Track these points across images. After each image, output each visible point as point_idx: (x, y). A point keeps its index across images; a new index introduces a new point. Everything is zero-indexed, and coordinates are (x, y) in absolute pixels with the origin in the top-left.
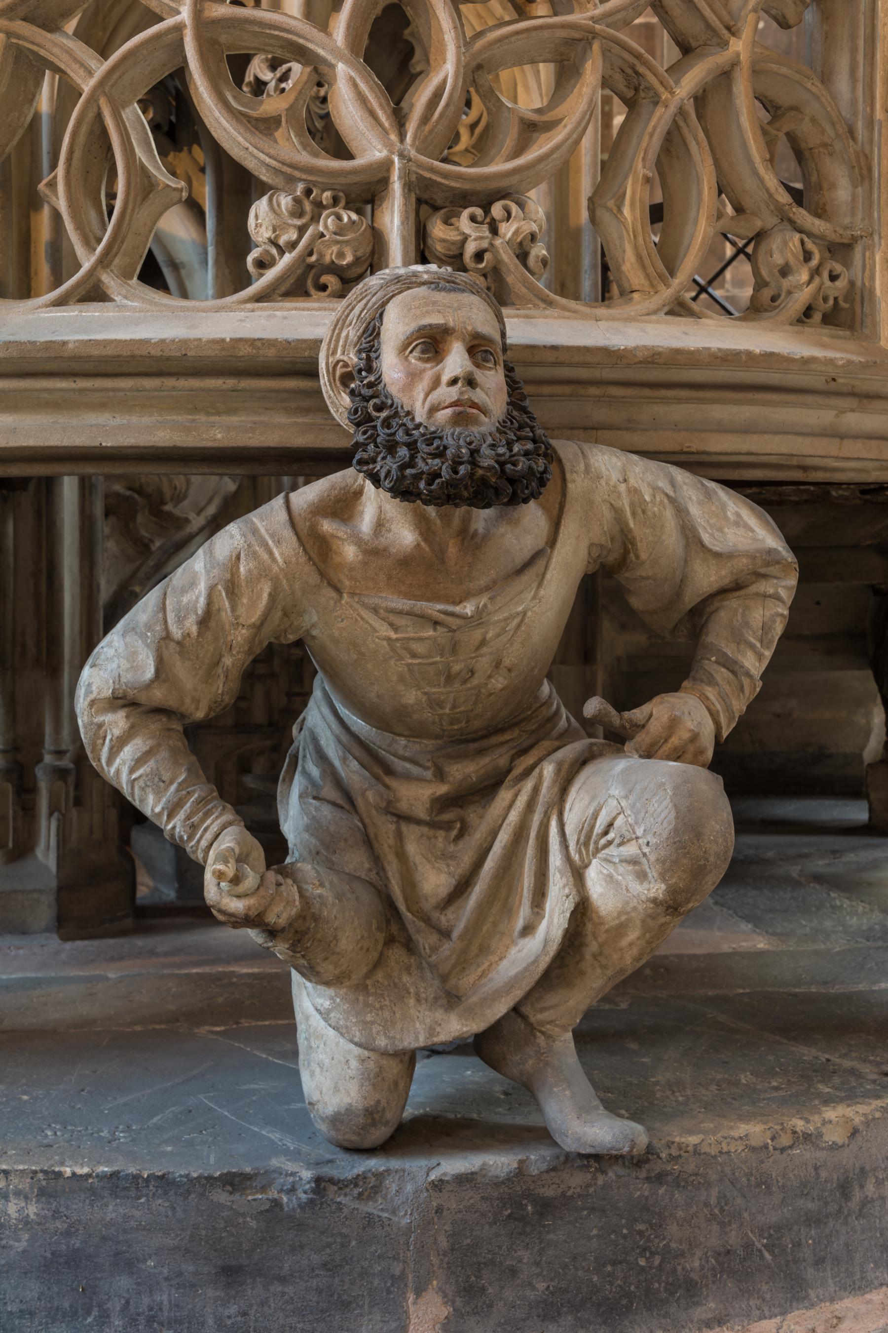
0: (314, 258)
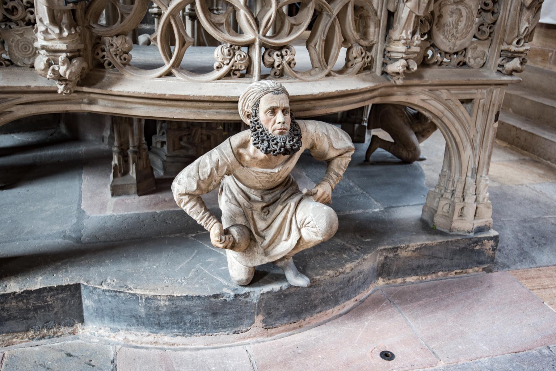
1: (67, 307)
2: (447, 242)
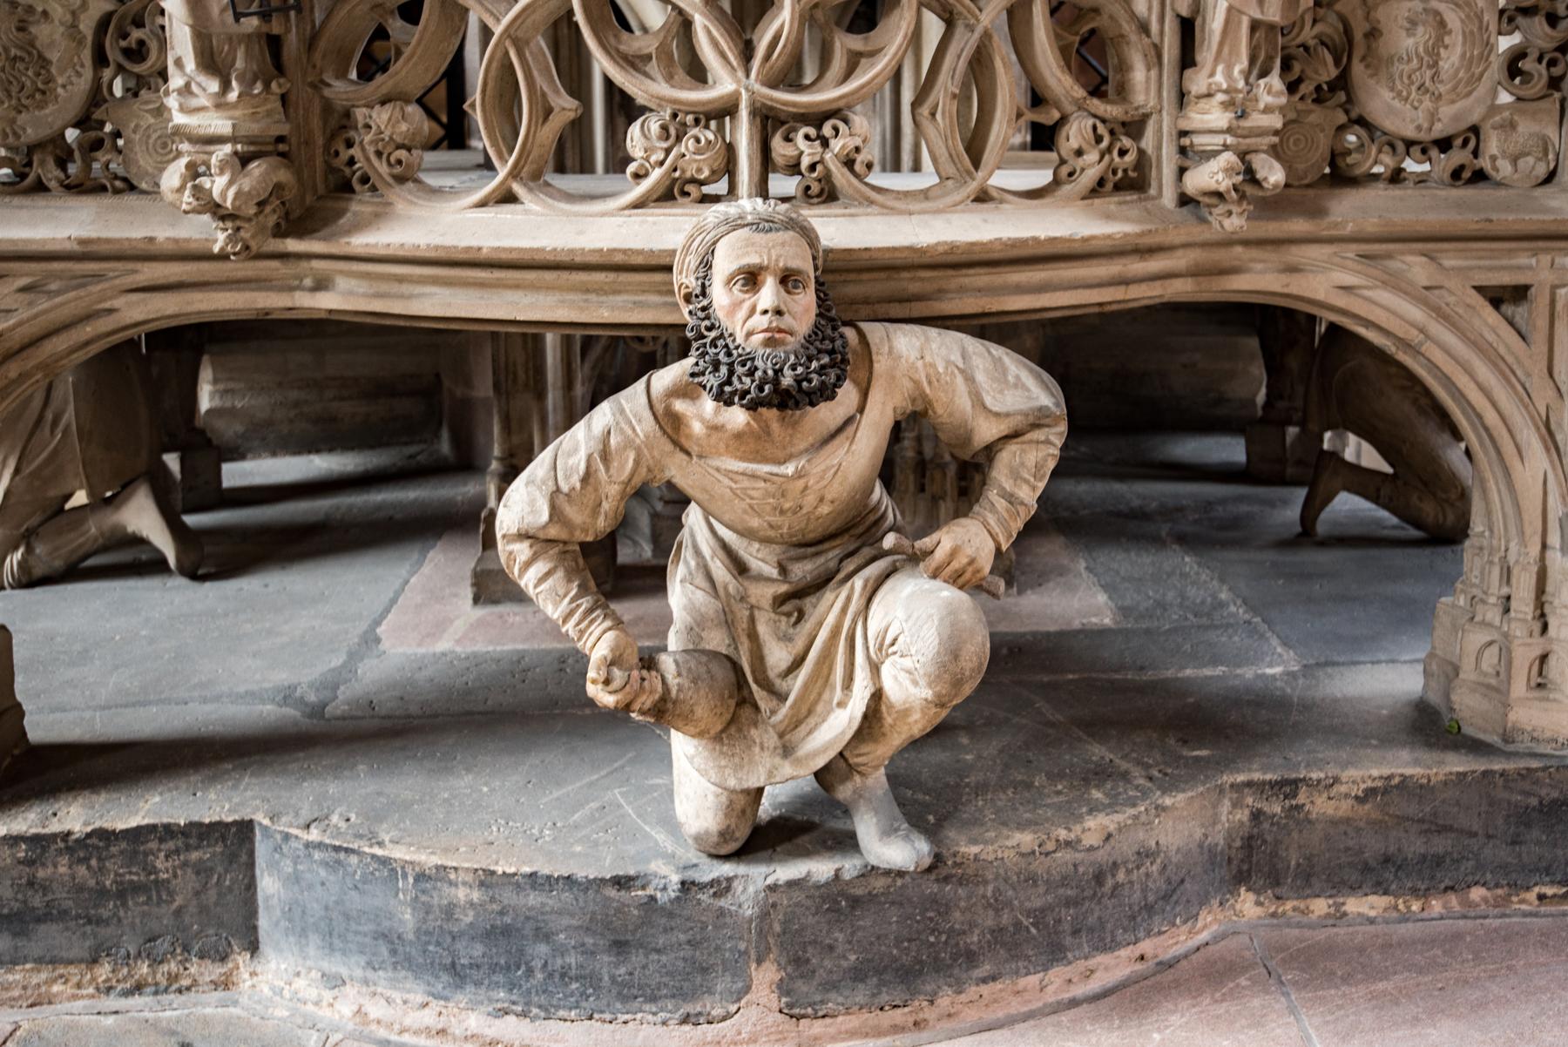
0: (677, 174)
1: (212, 894)
2: (1485, 773)
